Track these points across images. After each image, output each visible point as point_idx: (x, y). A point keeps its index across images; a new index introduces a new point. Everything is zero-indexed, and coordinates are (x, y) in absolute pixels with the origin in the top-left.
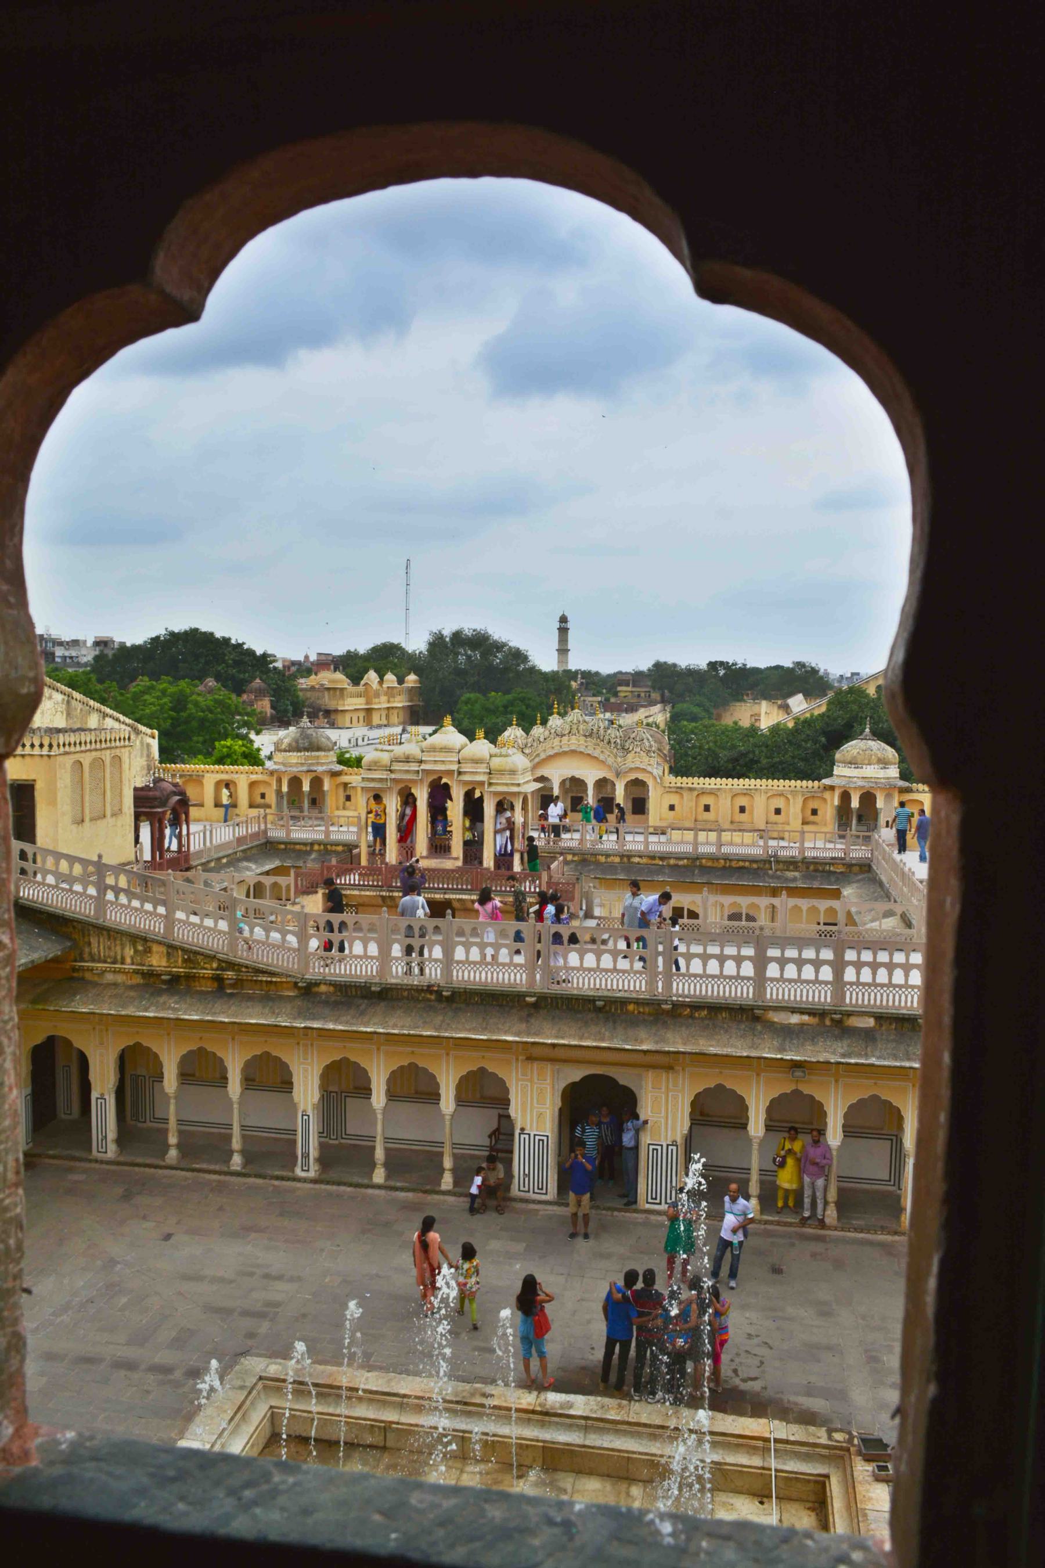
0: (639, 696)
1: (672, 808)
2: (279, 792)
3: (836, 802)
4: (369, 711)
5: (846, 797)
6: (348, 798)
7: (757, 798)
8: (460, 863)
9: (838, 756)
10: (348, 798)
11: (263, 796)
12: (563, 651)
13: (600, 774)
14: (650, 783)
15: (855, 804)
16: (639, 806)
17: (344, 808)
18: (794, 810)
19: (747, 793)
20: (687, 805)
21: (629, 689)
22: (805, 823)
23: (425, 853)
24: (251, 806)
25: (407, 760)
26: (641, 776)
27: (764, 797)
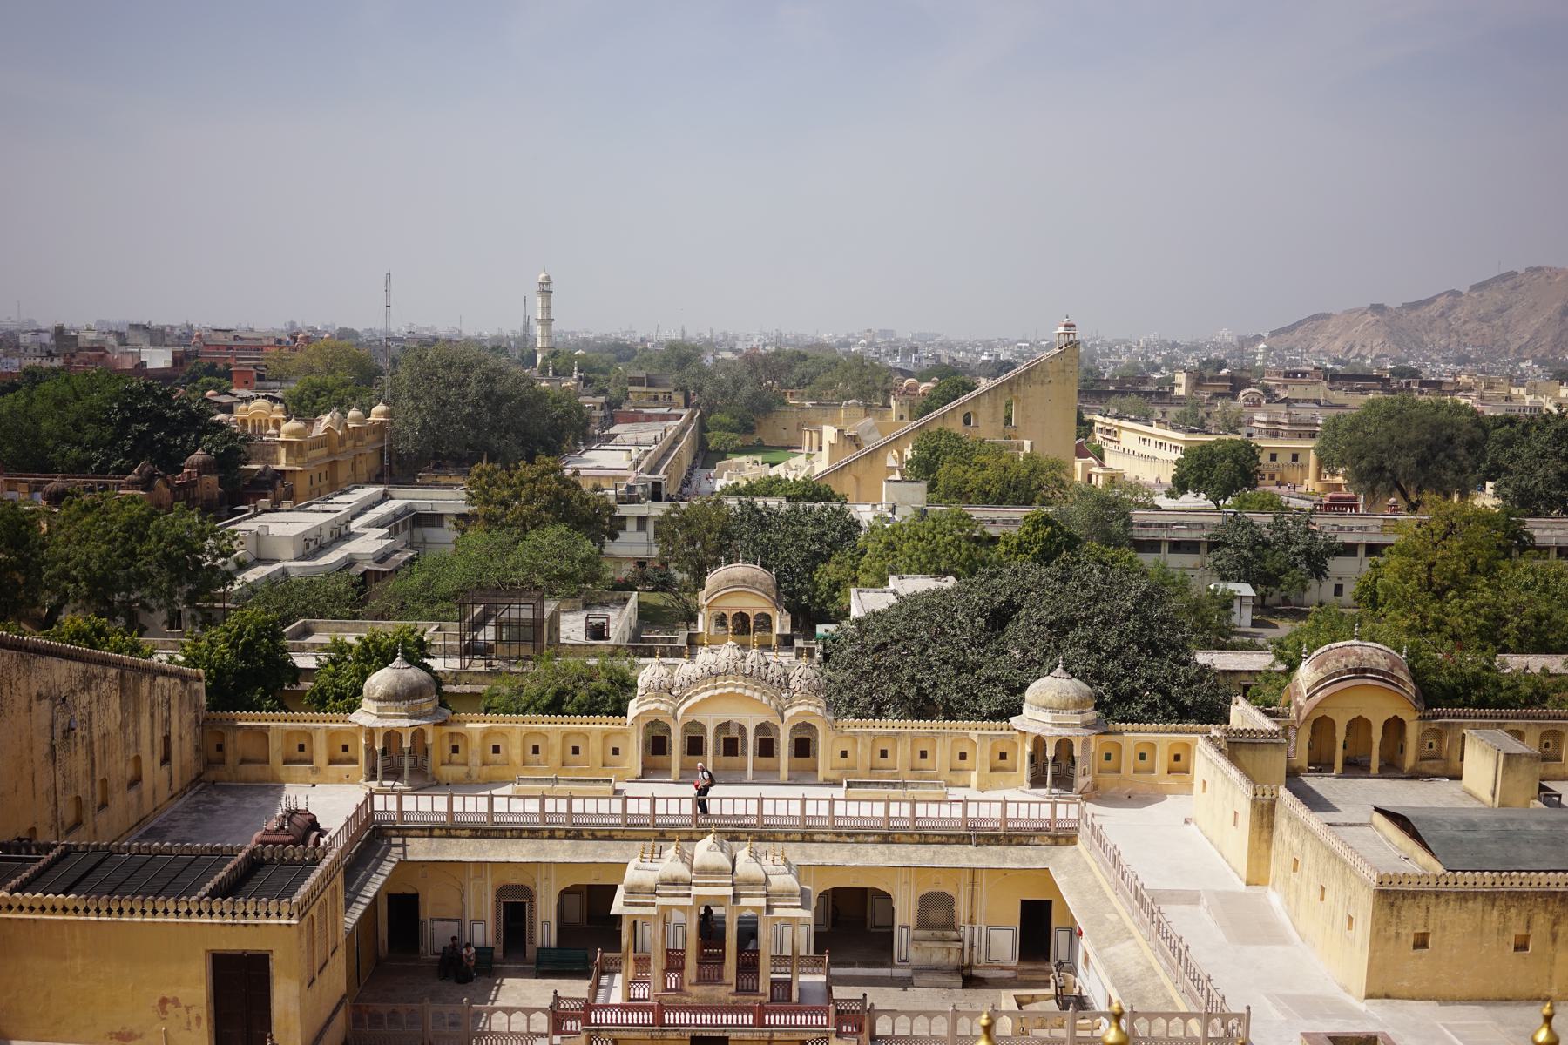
0: (656, 398)
1: (844, 754)
2: (370, 748)
3: (1028, 749)
4: (333, 464)
5: (1039, 742)
6: (455, 750)
7: (939, 742)
8: (733, 989)
9: (1028, 694)
10: (455, 750)
11: (345, 748)
12: (547, 322)
13: (762, 719)
14: (820, 728)
15: (1050, 753)
16: (803, 747)
17: (450, 763)
18: (980, 758)
19: (933, 737)
20: (863, 755)
21: (644, 389)
22: (992, 770)
23: (694, 980)
24: (331, 762)
25: (675, 882)
26: (809, 720)
27: (948, 741)
